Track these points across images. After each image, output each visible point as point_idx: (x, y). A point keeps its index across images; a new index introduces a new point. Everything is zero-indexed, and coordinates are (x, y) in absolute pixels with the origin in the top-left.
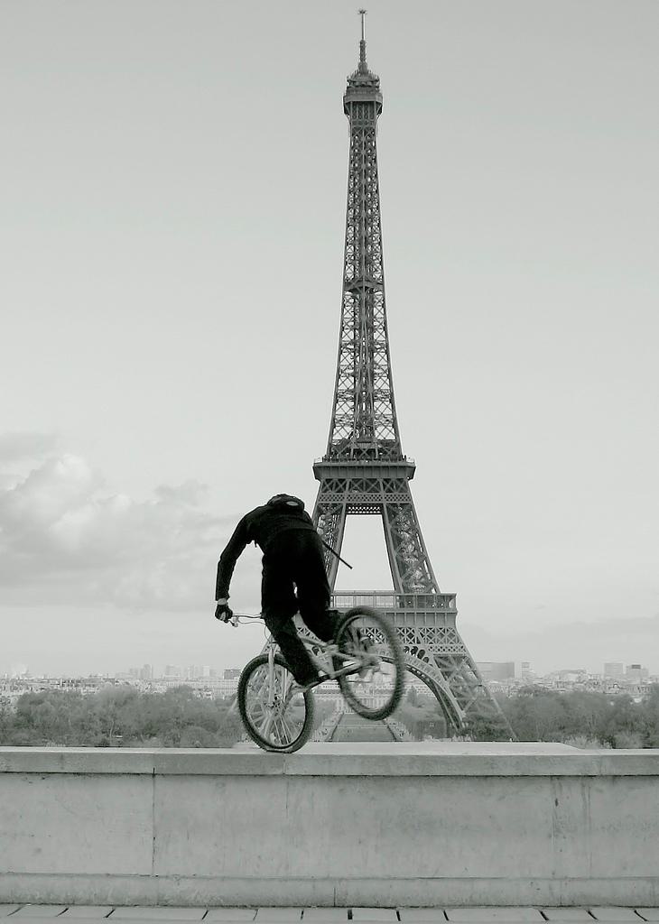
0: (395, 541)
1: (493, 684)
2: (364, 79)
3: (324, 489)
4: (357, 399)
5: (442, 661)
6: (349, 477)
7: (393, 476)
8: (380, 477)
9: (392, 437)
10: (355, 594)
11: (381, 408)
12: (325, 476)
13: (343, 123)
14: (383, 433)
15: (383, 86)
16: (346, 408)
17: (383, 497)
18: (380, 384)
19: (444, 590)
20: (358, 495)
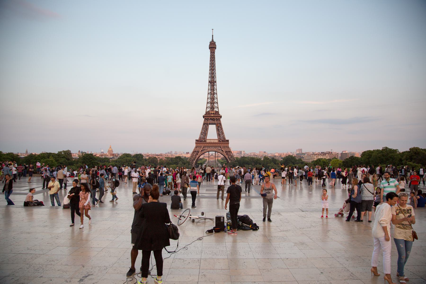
0: (218, 130)
1: (235, 155)
2: (213, 43)
3: (205, 120)
4: (211, 103)
5: (226, 152)
6: (209, 118)
7: (218, 118)
8: (215, 118)
9: (217, 111)
10: (210, 140)
11: (216, 105)
12: (205, 118)
13: (209, 50)
14: (216, 109)
15: (216, 44)
16: (209, 105)
17: (216, 122)
18: (215, 100)
19: (227, 139)
20: (211, 121)
